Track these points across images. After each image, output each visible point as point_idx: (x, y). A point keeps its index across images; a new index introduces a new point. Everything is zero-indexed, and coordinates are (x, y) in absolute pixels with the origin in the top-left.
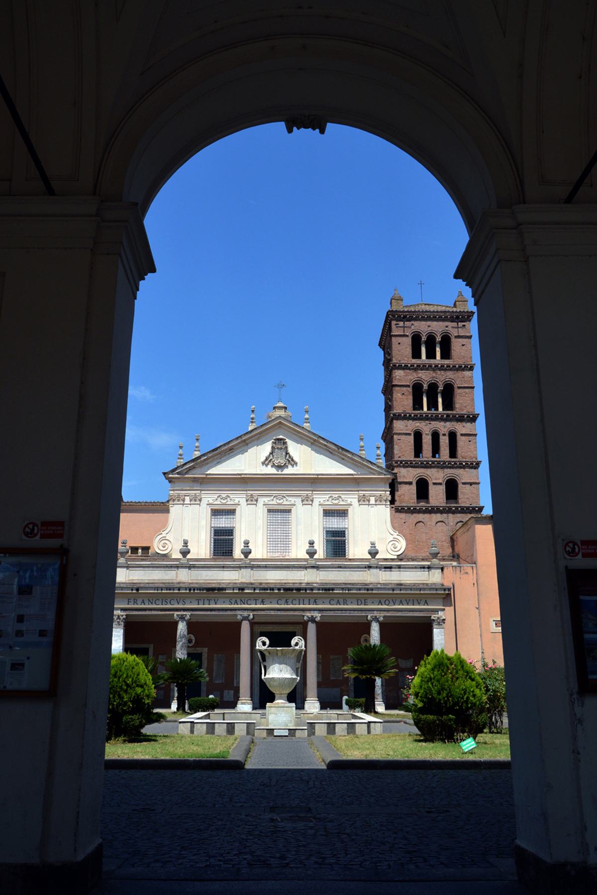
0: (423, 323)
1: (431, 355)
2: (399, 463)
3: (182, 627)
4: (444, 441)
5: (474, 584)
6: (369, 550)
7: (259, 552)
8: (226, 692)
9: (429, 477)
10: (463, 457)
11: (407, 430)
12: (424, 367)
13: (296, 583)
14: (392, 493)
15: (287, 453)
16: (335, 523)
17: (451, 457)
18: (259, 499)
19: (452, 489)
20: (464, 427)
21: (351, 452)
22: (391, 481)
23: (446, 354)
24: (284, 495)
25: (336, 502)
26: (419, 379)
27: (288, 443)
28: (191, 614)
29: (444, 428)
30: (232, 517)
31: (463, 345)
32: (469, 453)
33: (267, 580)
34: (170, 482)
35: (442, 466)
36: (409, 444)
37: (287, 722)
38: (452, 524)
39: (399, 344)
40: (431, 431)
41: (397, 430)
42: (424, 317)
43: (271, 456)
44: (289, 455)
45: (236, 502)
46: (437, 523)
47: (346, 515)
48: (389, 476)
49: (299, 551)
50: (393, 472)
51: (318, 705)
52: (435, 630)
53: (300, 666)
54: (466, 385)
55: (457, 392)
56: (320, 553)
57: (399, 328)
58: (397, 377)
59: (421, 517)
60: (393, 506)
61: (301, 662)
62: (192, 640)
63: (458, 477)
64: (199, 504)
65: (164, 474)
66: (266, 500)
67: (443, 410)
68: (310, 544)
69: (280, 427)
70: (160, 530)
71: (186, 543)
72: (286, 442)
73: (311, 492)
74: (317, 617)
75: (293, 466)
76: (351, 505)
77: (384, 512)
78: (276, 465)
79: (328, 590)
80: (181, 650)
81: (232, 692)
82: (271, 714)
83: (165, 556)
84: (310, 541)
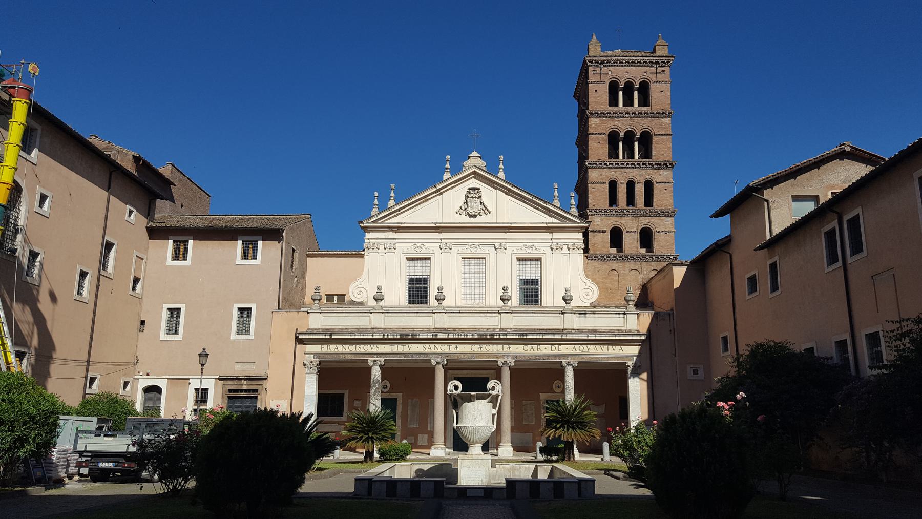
0: (622, 68)
1: (628, 102)
3: (376, 373)
4: (640, 190)
5: (671, 331)
6: (563, 296)
8: (420, 436)
9: (623, 226)
10: (658, 206)
11: (601, 179)
12: (621, 114)
13: (490, 329)
14: (586, 241)
16: (530, 272)
17: (646, 206)
19: (646, 237)
20: (660, 175)
23: (645, 100)
24: (478, 244)
26: (615, 127)
29: (640, 176)
31: (661, 91)
32: (665, 202)
35: (636, 215)
38: (646, 272)
40: (626, 179)
42: (622, 63)
44: (484, 204)
45: (431, 251)
48: (583, 225)
50: (587, 221)
51: (511, 449)
54: (664, 133)
55: (655, 139)
57: (597, 75)
58: (593, 125)
59: (615, 265)
60: (586, 254)
62: (387, 386)
66: (460, 248)
67: (639, 158)
71: (379, 289)
75: (486, 215)
79: (522, 337)
83: (360, 304)
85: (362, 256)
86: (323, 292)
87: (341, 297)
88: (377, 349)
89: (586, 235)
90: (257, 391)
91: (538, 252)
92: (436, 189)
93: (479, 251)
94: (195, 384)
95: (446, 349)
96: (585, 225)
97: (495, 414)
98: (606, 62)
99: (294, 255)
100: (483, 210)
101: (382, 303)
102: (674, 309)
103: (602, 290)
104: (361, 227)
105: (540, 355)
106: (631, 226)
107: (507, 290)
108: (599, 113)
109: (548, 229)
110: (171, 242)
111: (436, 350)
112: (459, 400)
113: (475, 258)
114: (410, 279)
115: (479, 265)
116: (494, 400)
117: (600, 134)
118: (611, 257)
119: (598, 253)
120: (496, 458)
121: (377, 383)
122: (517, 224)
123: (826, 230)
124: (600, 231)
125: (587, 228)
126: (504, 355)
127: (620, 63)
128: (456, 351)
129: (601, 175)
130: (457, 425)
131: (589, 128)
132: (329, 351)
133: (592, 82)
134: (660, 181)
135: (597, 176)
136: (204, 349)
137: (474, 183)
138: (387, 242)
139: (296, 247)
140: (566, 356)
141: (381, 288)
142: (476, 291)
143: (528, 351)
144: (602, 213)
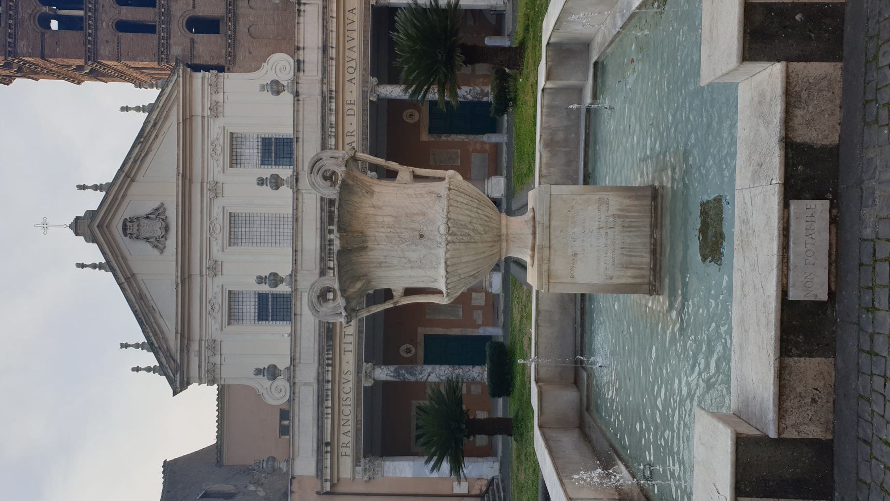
2: (163, 56)
3: (383, 373)
6: (272, 94)
8: (474, 303)
9: (185, 15)
14: (207, 68)
15: (147, 217)
16: (252, 151)
18: (215, 259)
21: (144, 123)
22: (189, 69)
24: (209, 222)
25: (219, 149)
27: (131, 216)
28: (365, 361)
30: (240, 296)
33: (316, 250)
34: (189, 383)
37: (603, 218)
40: (114, 6)
43: (151, 240)
44: (150, 214)
45: (218, 290)
46: (251, 8)
47: (239, 136)
48: (181, 71)
53: (411, 168)
58: (30, 50)
59: (242, 29)
61: (393, 165)
62: (407, 349)
64: (221, 341)
65: (175, 393)
66: (216, 248)
68: (262, 184)
69: (108, 226)
71: (259, 372)
72: (130, 218)
73: (205, 184)
76: (224, 127)
77: (232, 81)
78: (164, 233)
80: (416, 374)
81: (474, 295)
82: (572, 277)
84: (258, 184)
88: (349, 373)
89: (196, 68)
91: (222, 137)
96: (182, 67)
109: (187, 120)
114: (259, 319)
115: (240, 222)
117: (43, 41)
119: (224, 51)
121: (398, 372)
122: (178, 166)
129: (107, 42)
141: (257, 369)
142: (278, 226)
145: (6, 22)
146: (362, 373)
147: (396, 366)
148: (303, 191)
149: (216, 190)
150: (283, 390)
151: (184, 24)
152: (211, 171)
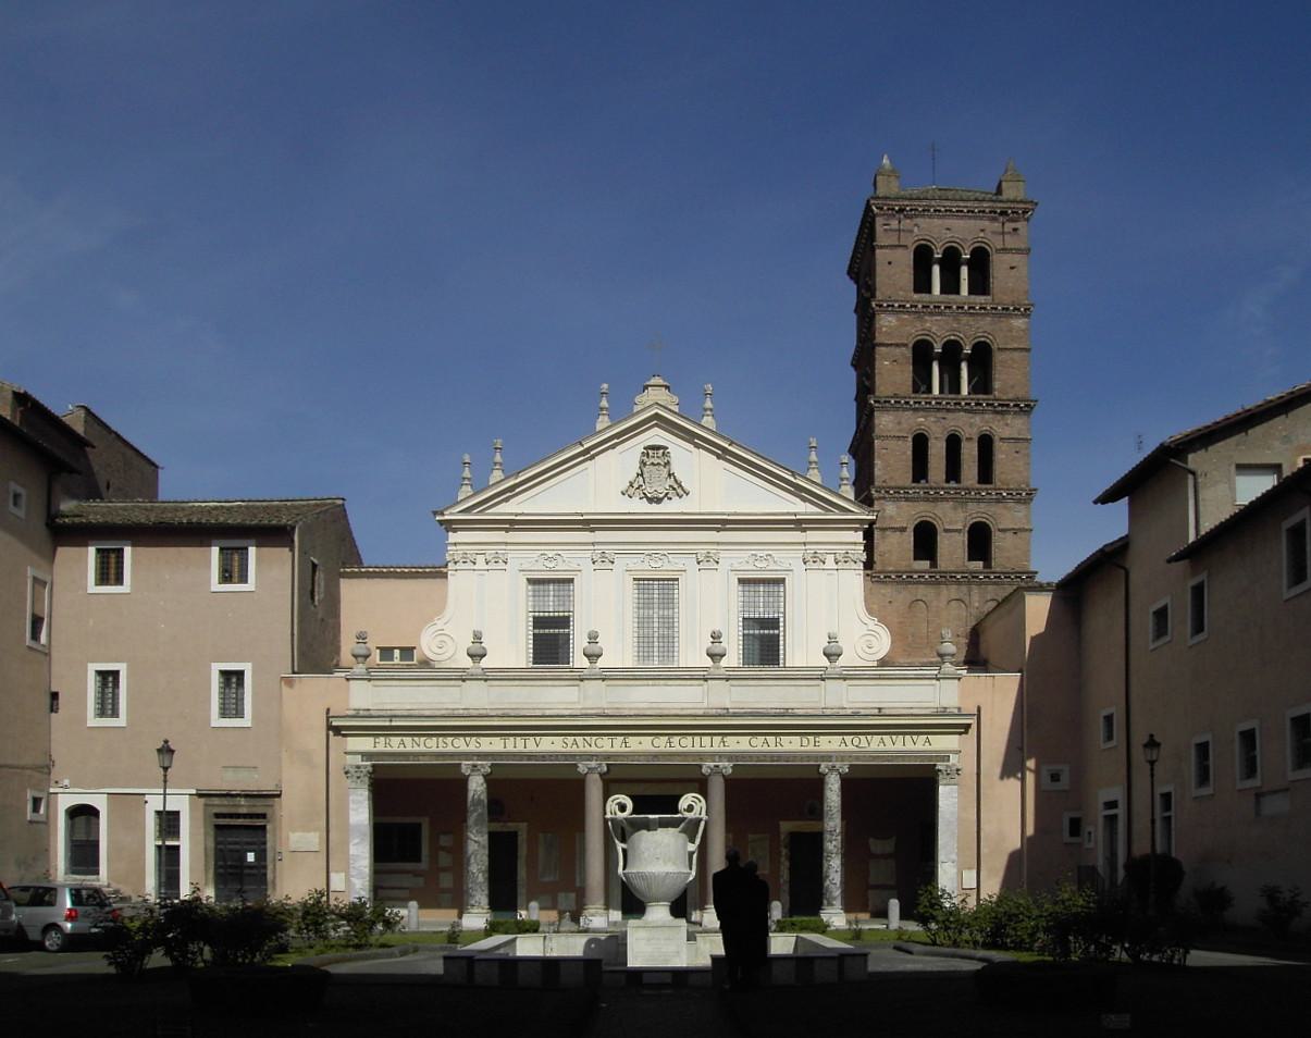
0: (937, 221)
1: (950, 286)
3: (477, 786)
4: (970, 452)
7: (619, 652)
11: (900, 431)
12: (936, 310)
14: (869, 547)
19: (980, 540)
20: (1007, 425)
23: (980, 285)
25: (763, 565)
27: (672, 455)
28: (492, 764)
29: (970, 426)
31: (1012, 268)
35: (961, 500)
36: (904, 457)
39: (890, 263)
41: (882, 430)
42: (940, 211)
44: (675, 477)
49: (692, 655)
52: (942, 789)
54: (1016, 346)
55: (998, 358)
56: (733, 658)
57: (890, 233)
58: (884, 329)
60: (869, 572)
63: (991, 519)
67: (969, 393)
69: (656, 425)
70: (431, 619)
74: (725, 768)
75: (681, 497)
77: (854, 581)
85: (445, 576)
86: (373, 644)
87: (407, 652)
89: (869, 535)
90: (264, 816)
91: (779, 568)
92: (582, 449)
93: (665, 567)
94: (154, 804)
95: (605, 745)
97: (693, 853)
98: (908, 208)
99: (316, 578)
100: (674, 489)
101: (485, 663)
102: (1024, 669)
103: (898, 636)
104: (441, 522)
105: (779, 756)
106: (953, 522)
107: (720, 637)
108: (896, 305)
109: (799, 524)
110: (92, 550)
111: (588, 748)
112: (628, 829)
113: (659, 580)
116: (691, 829)
117: (897, 345)
118: (915, 576)
119: (891, 569)
120: (698, 928)
123: (1289, 526)
124: (895, 529)
125: (872, 523)
126: (712, 756)
127: (935, 211)
128: (624, 749)
130: (626, 871)
131: (877, 334)
132: (389, 749)
133: (882, 247)
134: (1007, 436)
135: (891, 425)
136: (166, 742)
137: (656, 436)
138: (490, 551)
139: (318, 559)
140: (827, 757)
143: (759, 748)
144: (898, 494)
145: (919, 302)
146: (478, 760)
147: (486, 801)
148: (705, 687)
149: (707, 561)
150: (440, 651)
151: (925, 519)
152: (735, 554)
